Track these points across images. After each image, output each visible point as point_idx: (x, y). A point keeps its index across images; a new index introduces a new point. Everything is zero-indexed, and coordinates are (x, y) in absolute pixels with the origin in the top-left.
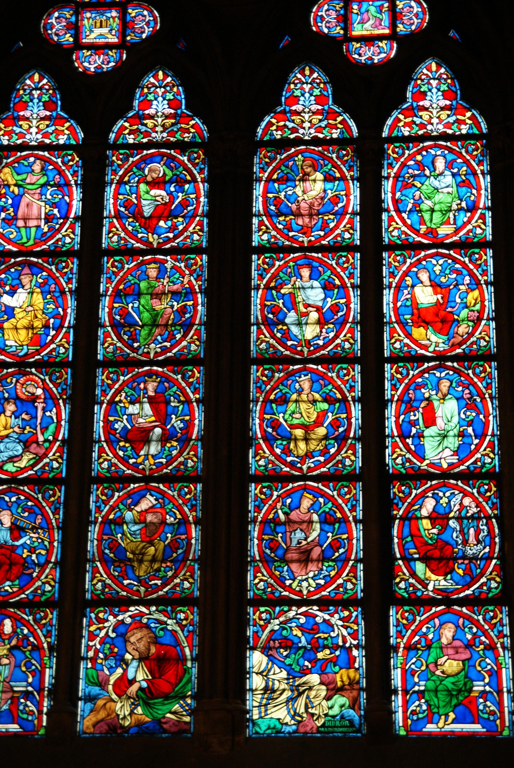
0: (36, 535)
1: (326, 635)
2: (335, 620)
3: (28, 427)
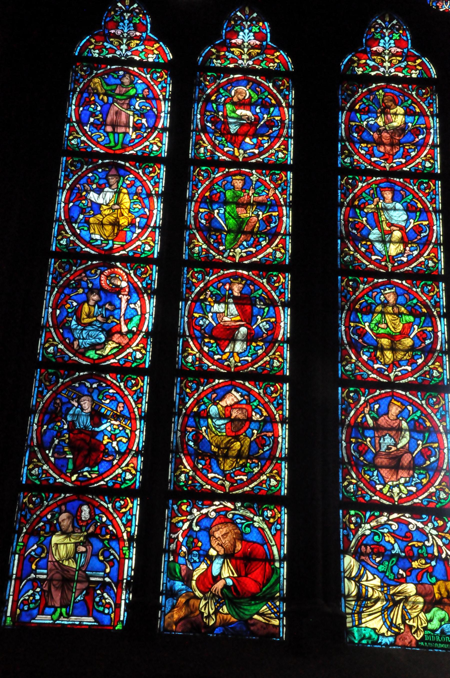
0: (118, 423)
1: (420, 544)
2: (429, 528)
3: (111, 317)
